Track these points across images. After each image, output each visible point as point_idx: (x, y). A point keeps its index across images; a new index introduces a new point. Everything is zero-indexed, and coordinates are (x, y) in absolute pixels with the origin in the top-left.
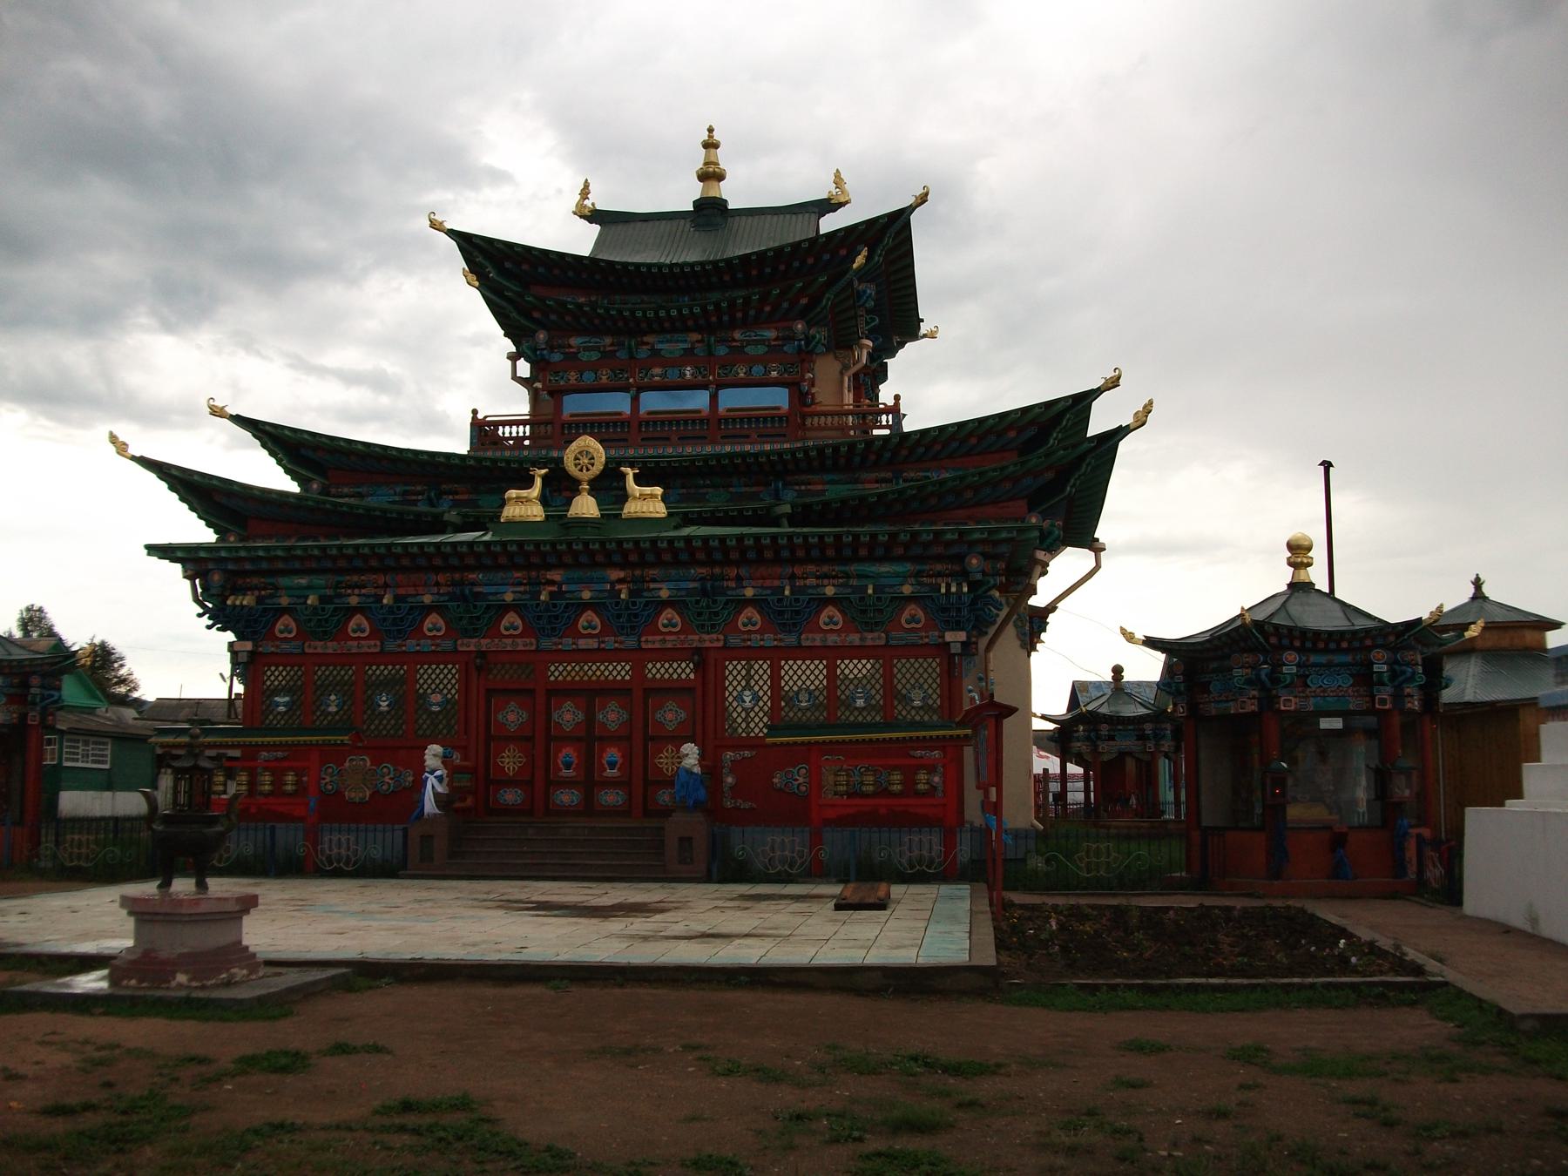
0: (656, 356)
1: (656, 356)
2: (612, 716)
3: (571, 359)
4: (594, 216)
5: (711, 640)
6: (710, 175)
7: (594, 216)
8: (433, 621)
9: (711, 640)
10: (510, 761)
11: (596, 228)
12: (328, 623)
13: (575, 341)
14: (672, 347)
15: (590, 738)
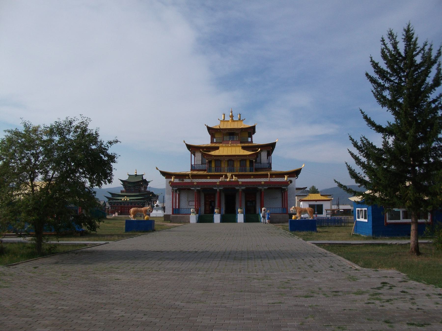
0: (131, 188)
1: (131, 188)
2: (127, 209)
3: (126, 188)
4: (129, 175)
5: (131, 205)
6: (136, 172)
7: (129, 175)
8: (119, 205)
9: (131, 205)
10: (123, 211)
11: (128, 176)
12: (114, 204)
13: (127, 187)
14: (132, 187)
15: (126, 210)
